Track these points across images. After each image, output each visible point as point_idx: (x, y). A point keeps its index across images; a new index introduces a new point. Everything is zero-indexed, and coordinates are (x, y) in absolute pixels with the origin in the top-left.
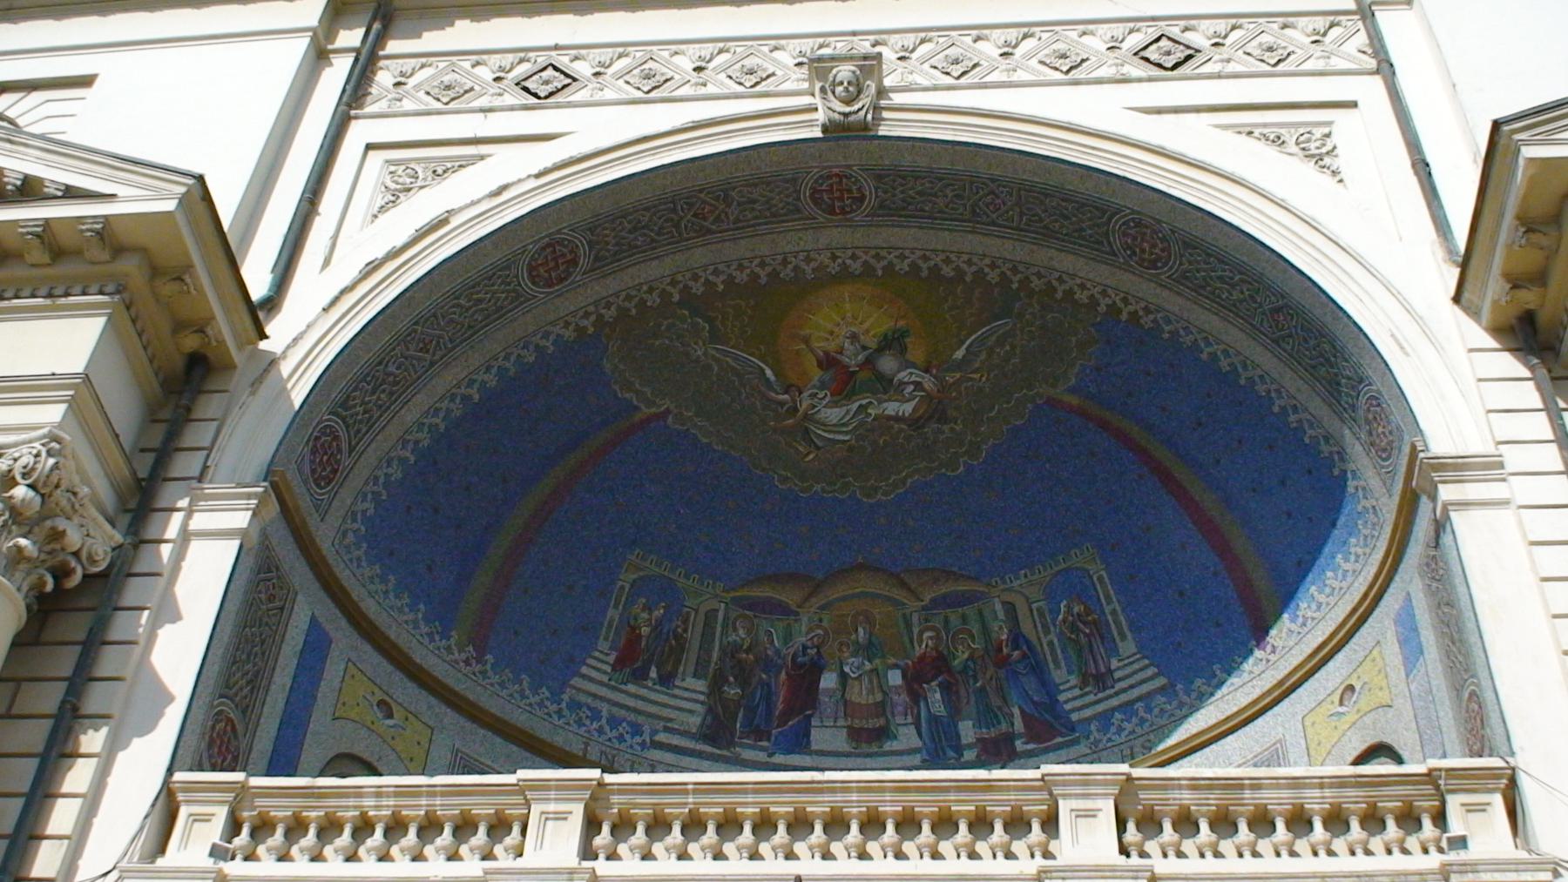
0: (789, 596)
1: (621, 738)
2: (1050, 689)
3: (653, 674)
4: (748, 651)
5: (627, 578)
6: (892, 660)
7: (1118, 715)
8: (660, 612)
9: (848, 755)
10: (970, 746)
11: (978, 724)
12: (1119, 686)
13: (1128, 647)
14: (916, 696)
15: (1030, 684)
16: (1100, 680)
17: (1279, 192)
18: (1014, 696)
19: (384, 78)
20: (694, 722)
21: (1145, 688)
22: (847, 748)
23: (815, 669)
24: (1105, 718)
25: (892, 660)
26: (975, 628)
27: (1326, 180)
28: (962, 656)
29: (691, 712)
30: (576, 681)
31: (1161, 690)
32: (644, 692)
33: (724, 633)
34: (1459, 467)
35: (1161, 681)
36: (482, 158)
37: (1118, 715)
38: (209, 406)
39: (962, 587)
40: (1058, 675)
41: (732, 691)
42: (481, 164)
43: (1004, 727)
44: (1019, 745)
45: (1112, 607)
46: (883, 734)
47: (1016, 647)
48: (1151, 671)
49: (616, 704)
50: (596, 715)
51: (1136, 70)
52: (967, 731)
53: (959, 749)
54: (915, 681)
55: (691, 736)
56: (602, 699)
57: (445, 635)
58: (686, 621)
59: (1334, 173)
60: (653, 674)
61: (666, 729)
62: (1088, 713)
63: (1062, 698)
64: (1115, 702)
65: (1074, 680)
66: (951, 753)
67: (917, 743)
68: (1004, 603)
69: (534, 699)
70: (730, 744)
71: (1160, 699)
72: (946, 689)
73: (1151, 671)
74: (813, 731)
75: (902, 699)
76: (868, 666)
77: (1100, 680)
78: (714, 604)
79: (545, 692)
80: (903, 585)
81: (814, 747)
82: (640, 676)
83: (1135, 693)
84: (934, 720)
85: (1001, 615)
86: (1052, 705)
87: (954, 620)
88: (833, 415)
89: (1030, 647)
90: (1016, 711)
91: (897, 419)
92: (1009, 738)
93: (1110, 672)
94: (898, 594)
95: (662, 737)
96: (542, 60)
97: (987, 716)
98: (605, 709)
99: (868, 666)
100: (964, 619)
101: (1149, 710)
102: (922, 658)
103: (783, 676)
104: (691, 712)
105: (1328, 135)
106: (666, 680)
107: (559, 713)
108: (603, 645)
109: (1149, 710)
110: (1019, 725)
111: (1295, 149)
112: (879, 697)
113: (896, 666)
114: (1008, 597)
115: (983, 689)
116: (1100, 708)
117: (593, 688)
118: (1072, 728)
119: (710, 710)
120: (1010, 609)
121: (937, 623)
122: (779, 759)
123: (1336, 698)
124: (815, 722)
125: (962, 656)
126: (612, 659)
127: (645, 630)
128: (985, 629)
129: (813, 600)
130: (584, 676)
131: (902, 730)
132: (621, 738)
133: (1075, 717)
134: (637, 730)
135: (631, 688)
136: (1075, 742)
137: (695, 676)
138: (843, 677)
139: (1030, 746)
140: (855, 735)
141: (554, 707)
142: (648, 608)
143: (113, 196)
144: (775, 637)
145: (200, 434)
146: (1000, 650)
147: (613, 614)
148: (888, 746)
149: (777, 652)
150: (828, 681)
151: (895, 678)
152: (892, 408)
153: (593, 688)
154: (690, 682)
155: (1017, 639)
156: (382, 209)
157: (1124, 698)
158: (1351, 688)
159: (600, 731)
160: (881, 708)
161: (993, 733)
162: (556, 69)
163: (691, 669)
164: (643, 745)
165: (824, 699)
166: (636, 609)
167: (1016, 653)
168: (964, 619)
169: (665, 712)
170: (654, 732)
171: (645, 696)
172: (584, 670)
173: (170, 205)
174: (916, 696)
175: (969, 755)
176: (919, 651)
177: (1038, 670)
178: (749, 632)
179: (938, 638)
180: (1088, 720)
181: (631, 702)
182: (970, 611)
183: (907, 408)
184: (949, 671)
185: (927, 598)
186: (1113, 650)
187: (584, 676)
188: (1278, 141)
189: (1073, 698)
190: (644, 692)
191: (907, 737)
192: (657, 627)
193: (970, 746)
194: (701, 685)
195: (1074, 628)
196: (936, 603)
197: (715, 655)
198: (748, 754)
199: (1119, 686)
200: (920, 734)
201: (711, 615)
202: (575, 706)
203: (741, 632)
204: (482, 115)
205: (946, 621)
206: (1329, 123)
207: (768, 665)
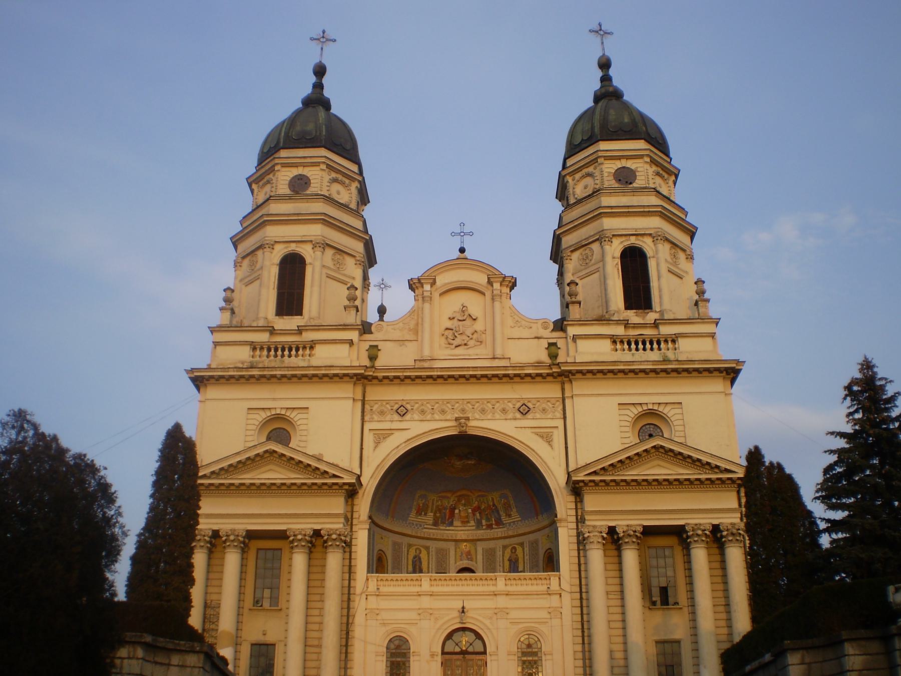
0: (449, 495)
1: (418, 528)
2: (500, 516)
3: (423, 513)
4: (441, 506)
5: (417, 497)
6: (469, 507)
7: (512, 524)
8: (424, 501)
9: (461, 527)
10: (484, 525)
11: (486, 521)
12: (513, 518)
13: (514, 510)
14: (474, 515)
15: (496, 515)
16: (510, 516)
17: (540, 455)
18: (493, 516)
19: (367, 406)
20: (431, 522)
21: (517, 519)
22: (460, 525)
23: (455, 509)
24: (510, 524)
25: (469, 507)
26: (486, 502)
27: (549, 448)
28: (483, 507)
29: (430, 520)
30: (410, 518)
31: (520, 521)
32: (421, 518)
33: (436, 503)
34: (561, 520)
35: (520, 519)
36: (392, 434)
37: (512, 524)
38: (356, 501)
39: (483, 493)
40: (501, 513)
41: (438, 515)
42: (392, 435)
43: (491, 522)
44: (494, 526)
45: (512, 502)
46: (468, 522)
47: (493, 506)
48: (518, 516)
49: (417, 521)
50: (413, 524)
51: (518, 415)
52: (484, 522)
53: (482, 526)
54: (474, 511)
55: (432, 525)
56: (414, 521)
57: (388, 518)
58: (429, 502)
59: (551, 446)
60: (423, 513)
61: (427, 525)
62: (506, 522)
63: (502, 518)
64: (512, 521)
65: (504, 515)
66: (481, 527)
67: (474, 524)
68: (492, 498)
69: (403, 524)
70: (439, 526)
71: (519, 522)
72: (480, 513)
73: (518, 516)
74: (454, 522)
75: (471, 515)
76: (464, 508)
77: (510, 516)
78: (434, 498)
79: (404, 522)
80: (471, 492)
81: (454, 525)
82: (420, 514)
83: (515, 520)
84: (477, 519)
85: (491, 500)
86: (500, 519)
87: (482, 500)
88: (459, 463)
89: (496, 507)
90: (493, 519)
91: (471, 464)
92: (492, 525)
93: (511, 514)
94: (471, 494)
95: (425, 526)
96: (400, 404)
97: (488, 520)
98: (415, 523)
99: (464, 508)
100: (483, 499)
101: (517, 524)
102: (475, 507)
103: (448, 511)
104: (430, 520)
105: (551, 435)
106: (425, 514)
107: (407, 526)
108: (413, 510)
109: (517, 524)
110: (494, 522)
111: (545, 440)
112: (467, 514)
113: (470, 508)
114: (492, 496)
115: (487, 514)
116: (509, 521)
117: (412, 519)
118: (504, 524)
119: (434, 519)
120: (493, 499)
121: (478, 500)
122: (448, 528)
123: (547, 535)
124: (454, 520)
125: (483, 507)
126: (415, 512)
127: (421, 505)
128: (488, 502)
129: (454, 496)
130: (411, 517)
131: (471, 522)
132: (418, 528)
133: (504, 522)
134: (421, 526)
135: (419, 517)
136: (504, 527)
137: (431, 512)
138: (460, 510)
139: (496, 527)
140: (462, 522)
141: (406, 525)
142: (422, 500)
143: (343, 478)
144: (446, 503)
145: (355, 508)
146: (490, 506)
147: (415, 503)
148: (469, 525)
149: (447, 506)
150: (457, 511)
151: (470, 511)
152: (470, 462)
153: (412, 519)
154: (430, 514)
155: (494, 505)
156: (376, 447)
157: (513, 520)
158: (548, 536)
159: (414, 527)
160: (467, 517)
161: (489, 523)
162: (404, 407)
163: (430, 511)
164: (422, 529)
165: (456, 515)
166: (419, 501)
167: (494, 508)
168: (483, 499)
169: (426, 521)
170: (424, 526)
171: (422, 518)
172: (411, 516)
173: (354, 481)
174: (474, 515)
175: (484, 527)
176: (475, 505)
177: (498, 512)
178: (441, 502)
179: (478, 503)
180: (506, 523)
181: (420, 520)
182: (485, 498)
183: (473, 462)
184: (480, 509)
185: (476, 495)
186: (512, 510)
187: (411, 517)
188: (542, 437)
189: (503, 518)
190: (421, 518)
191: (472, 523)
192: (423, 504)
193: (484, 525)
194: (432, 514)
195: (504, 504)
196: (479, 496)
197: (435, 507)
198: (442, 528)
199: (513, 518)
200: (475, 522)
201: (433, 500)
202: (409, 523)
203: (439, 502)
204: (390, 422)
205: (480, 500)
206: (552, 432)
207: (445, 509)
